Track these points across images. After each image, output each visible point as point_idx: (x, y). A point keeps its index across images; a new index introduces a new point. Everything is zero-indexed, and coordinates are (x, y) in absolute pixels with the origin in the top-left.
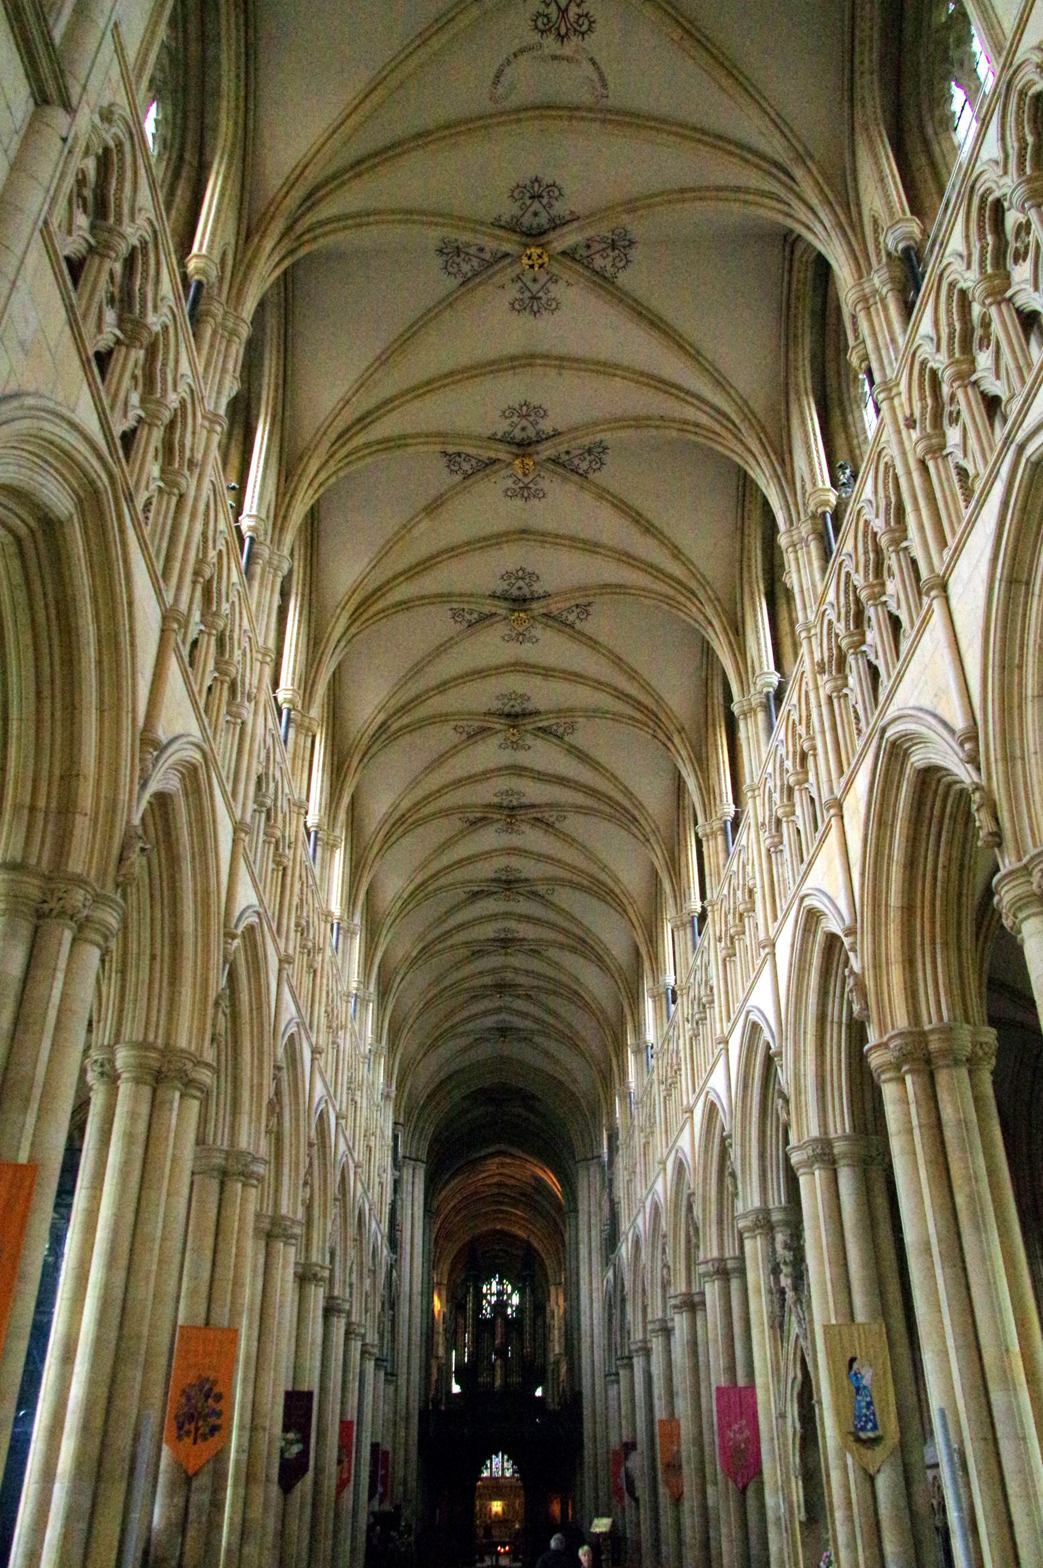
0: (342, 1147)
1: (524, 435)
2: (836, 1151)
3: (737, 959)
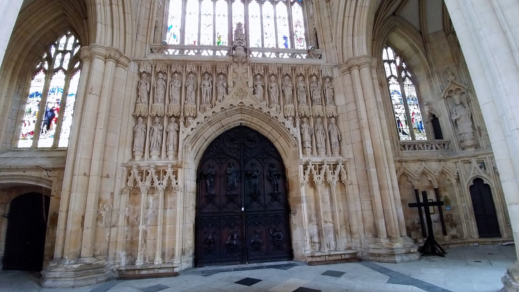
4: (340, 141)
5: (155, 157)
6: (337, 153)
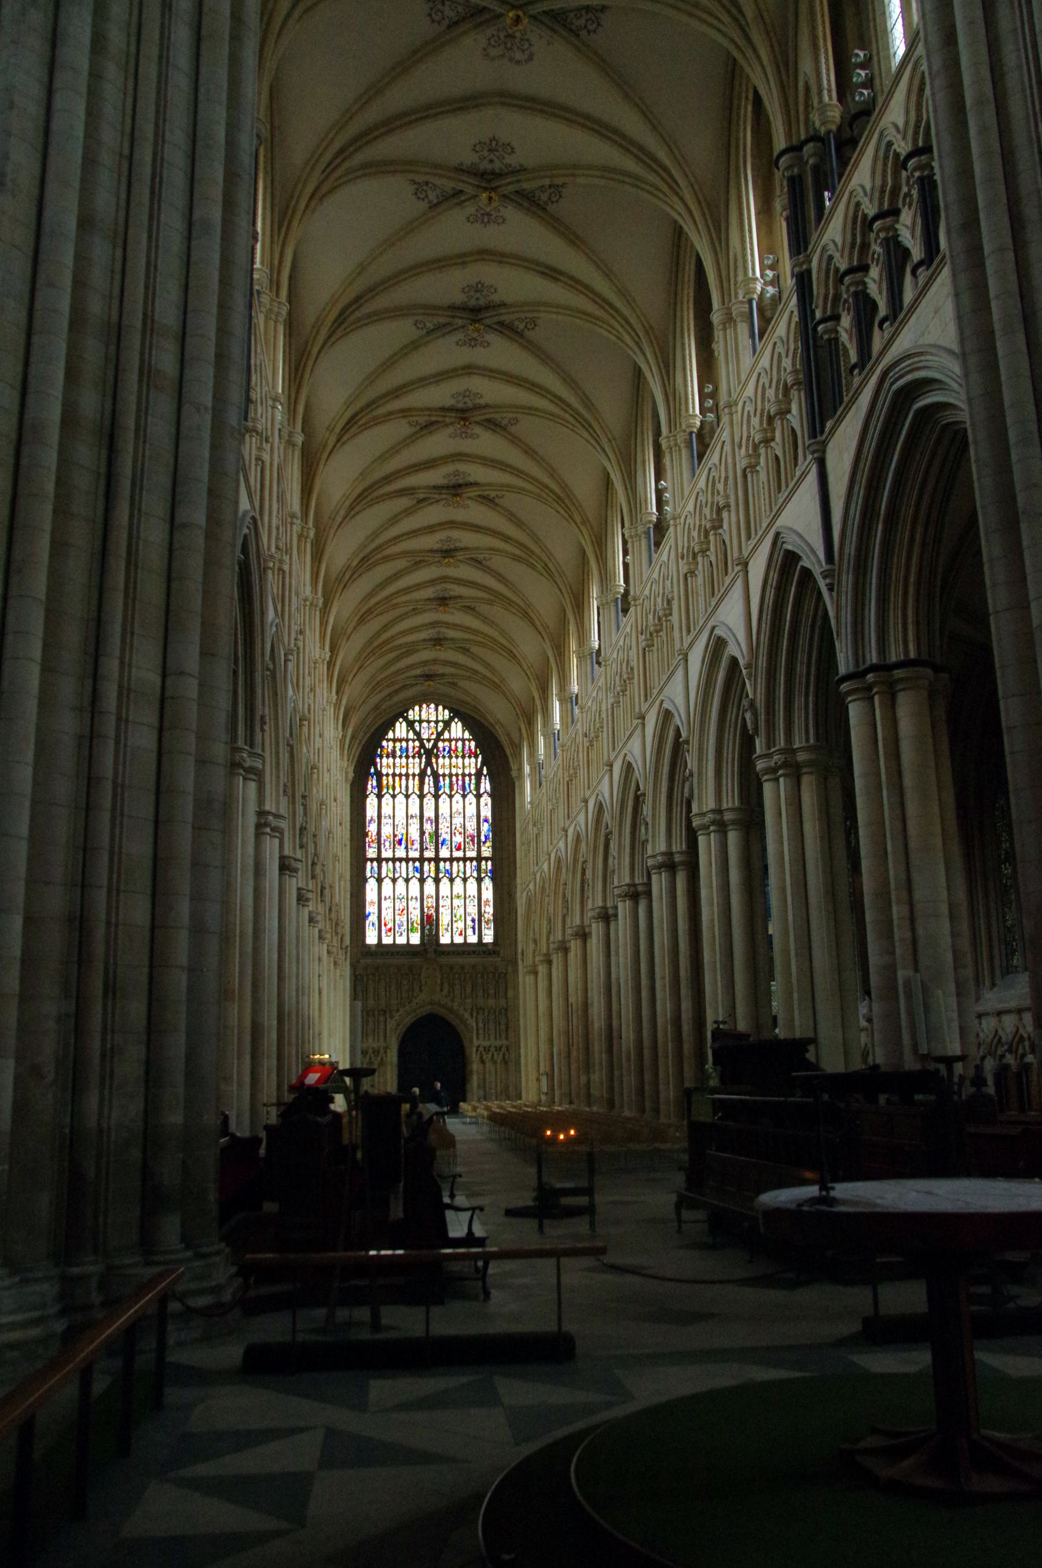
1: (489, 167)
3: (655, 648)
4: (507, 1028)
5: (370, 1041)
6: (503, 1037)
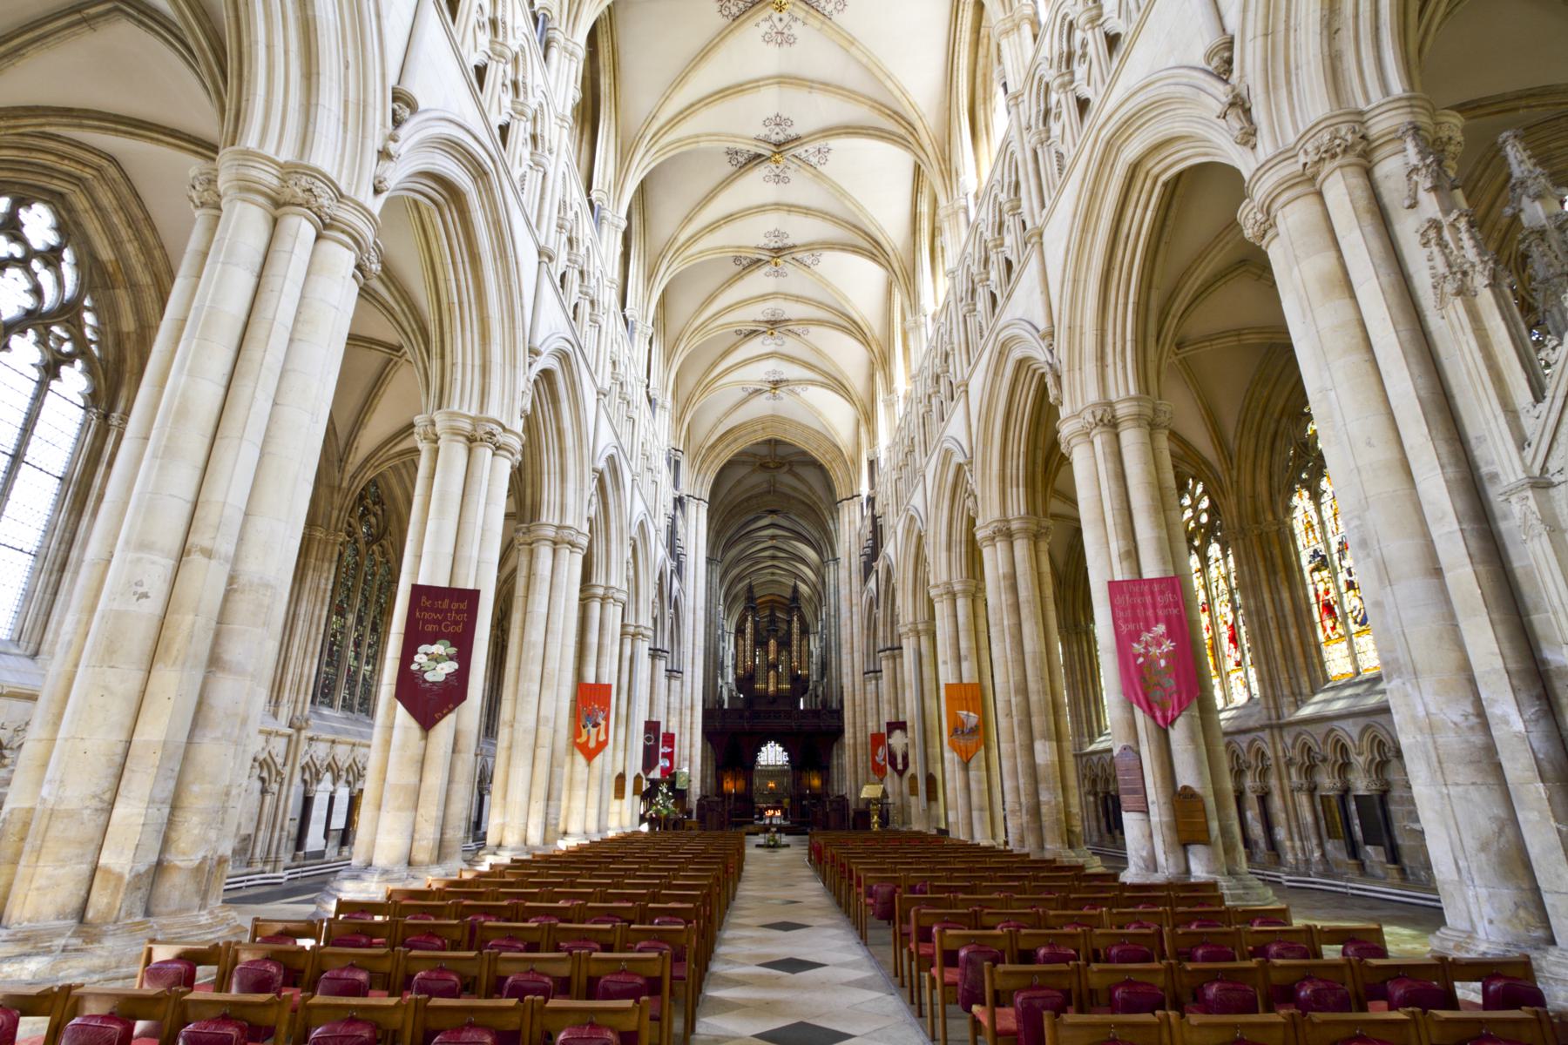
0: (639, 507)
2: (1119, 413)
